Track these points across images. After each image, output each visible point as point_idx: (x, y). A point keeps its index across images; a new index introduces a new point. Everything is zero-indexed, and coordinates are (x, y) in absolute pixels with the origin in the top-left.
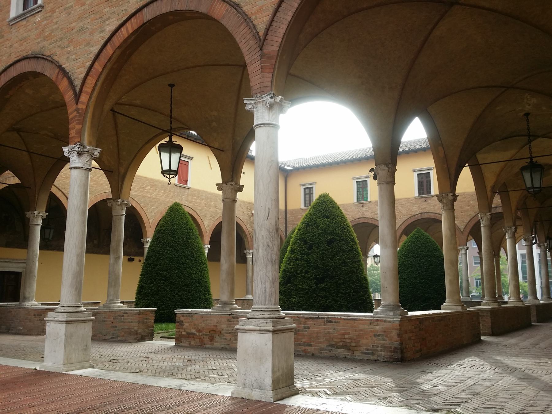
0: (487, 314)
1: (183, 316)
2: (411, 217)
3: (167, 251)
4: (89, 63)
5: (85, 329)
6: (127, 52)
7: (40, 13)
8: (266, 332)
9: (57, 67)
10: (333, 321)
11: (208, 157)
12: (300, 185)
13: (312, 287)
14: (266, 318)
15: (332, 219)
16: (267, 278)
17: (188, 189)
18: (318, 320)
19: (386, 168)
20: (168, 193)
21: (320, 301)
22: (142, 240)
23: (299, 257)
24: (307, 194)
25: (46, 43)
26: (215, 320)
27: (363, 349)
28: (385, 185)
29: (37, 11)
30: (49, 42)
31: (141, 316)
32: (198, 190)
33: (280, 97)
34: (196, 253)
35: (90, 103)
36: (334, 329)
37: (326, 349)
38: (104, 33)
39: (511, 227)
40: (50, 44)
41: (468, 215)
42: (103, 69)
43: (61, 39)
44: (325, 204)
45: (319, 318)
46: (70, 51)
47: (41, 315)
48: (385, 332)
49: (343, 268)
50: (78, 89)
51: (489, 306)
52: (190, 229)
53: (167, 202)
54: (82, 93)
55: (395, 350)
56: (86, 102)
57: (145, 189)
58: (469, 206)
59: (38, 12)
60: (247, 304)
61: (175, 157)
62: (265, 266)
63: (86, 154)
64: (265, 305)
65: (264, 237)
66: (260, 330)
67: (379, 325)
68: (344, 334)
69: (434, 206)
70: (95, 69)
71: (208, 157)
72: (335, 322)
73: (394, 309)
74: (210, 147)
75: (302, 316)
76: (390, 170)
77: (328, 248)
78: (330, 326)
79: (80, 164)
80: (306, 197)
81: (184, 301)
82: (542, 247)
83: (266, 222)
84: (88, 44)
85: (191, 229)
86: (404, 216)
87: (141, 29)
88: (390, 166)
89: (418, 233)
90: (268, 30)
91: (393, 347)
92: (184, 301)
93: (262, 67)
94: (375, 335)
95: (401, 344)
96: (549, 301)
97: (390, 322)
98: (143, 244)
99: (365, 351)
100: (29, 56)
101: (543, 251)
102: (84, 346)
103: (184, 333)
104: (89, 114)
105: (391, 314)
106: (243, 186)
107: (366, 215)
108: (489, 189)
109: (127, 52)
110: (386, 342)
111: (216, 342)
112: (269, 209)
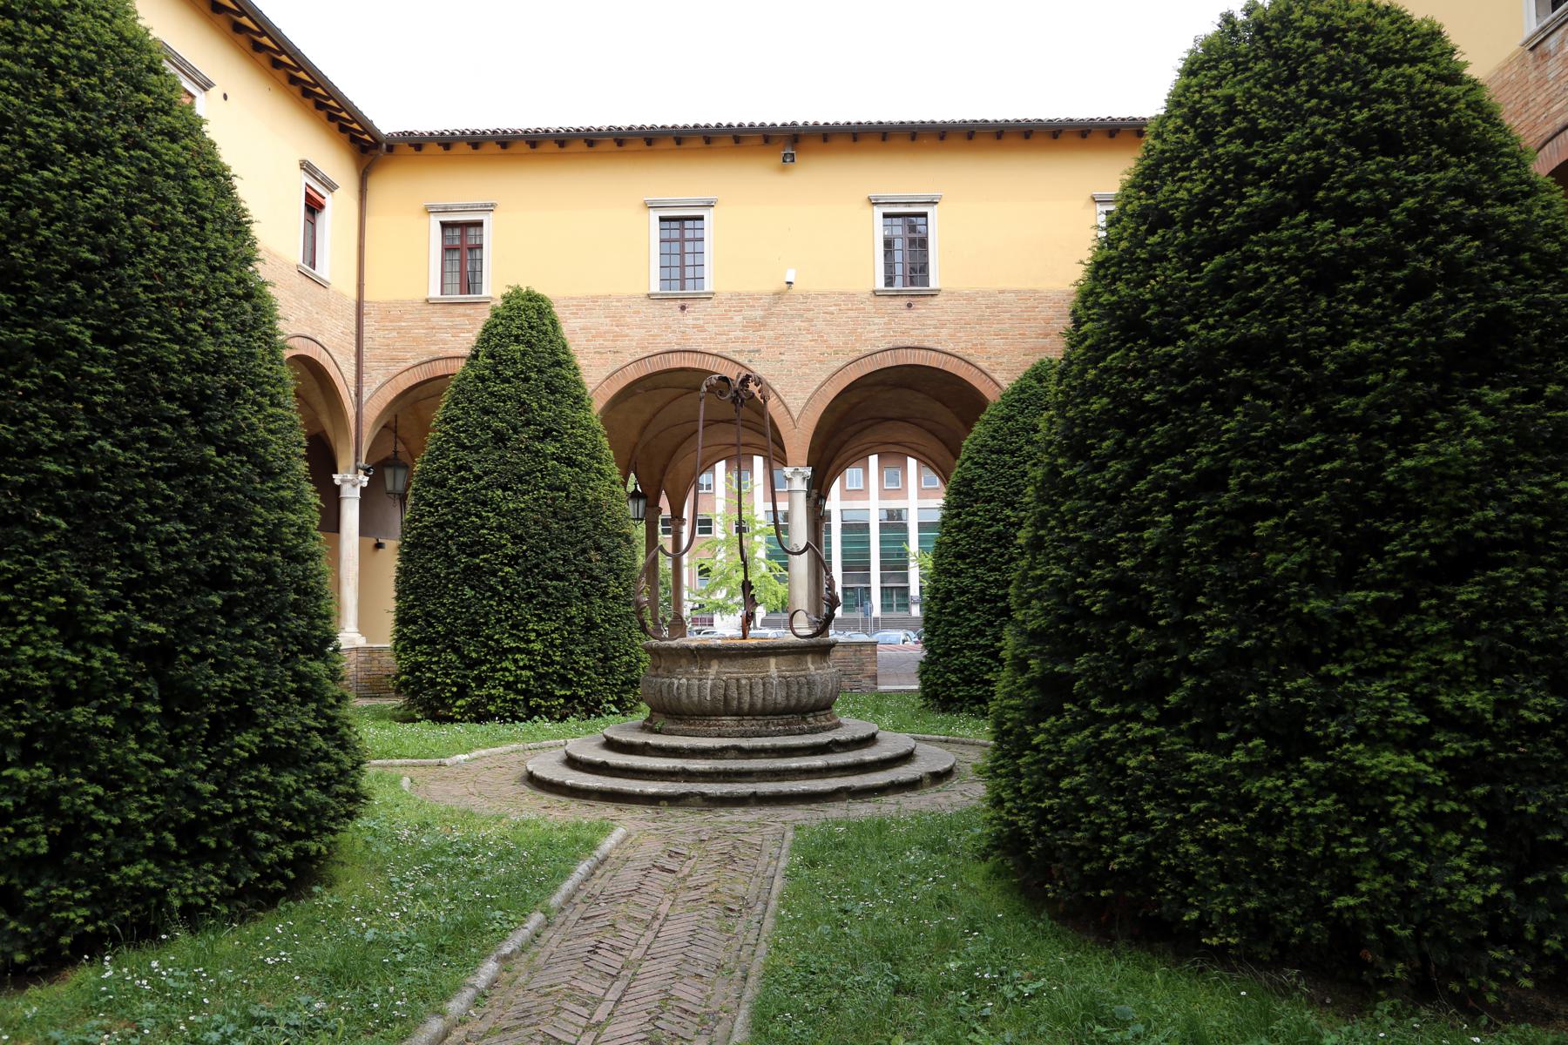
58: (1047, 335)
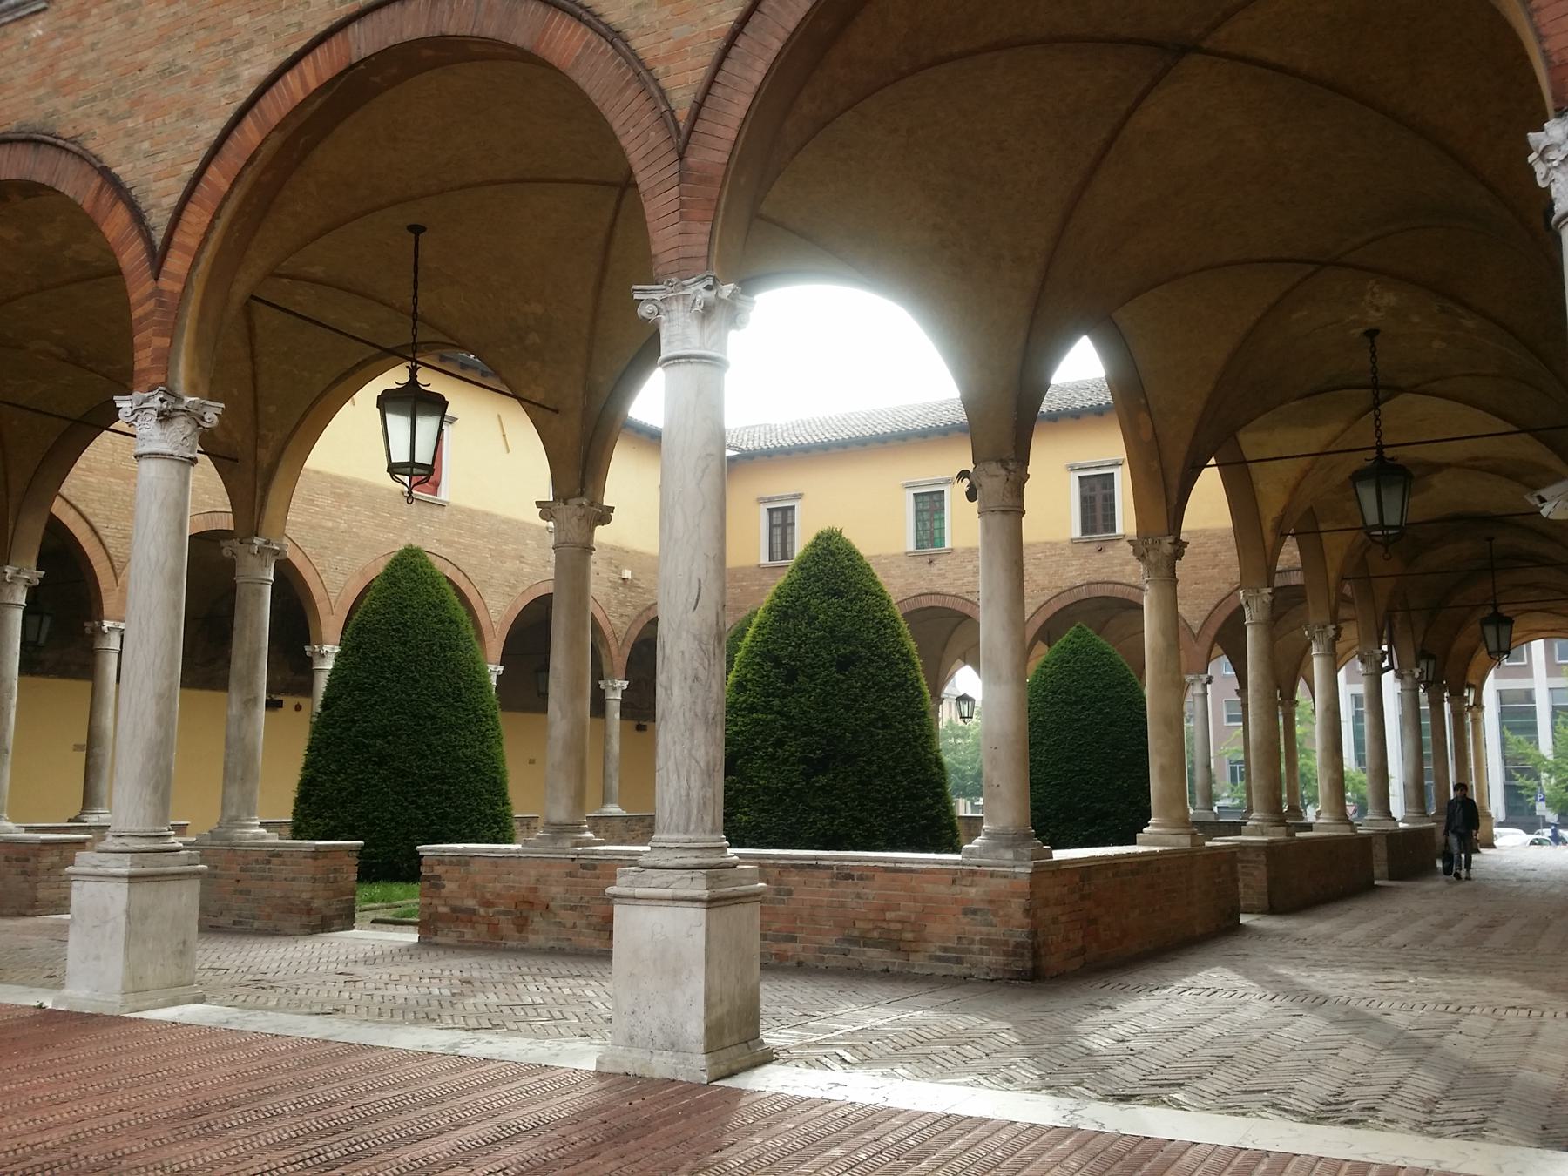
0: (1258, 856)
1: (441, 863)
2: (1060, 594)
3: (383, 682)
4: (194, 166)
5: (180, 896)
6: (302, 141)
7: (42, 15)
8: (689, 904)
9: (97, 172)
10: (856, 874)
11: (499, 416)
12: (758, 499)
13: (795, 783)
14: (689, 866)
15: (851, 601)
16: (693, 762)
17: (440, 508)
18: (816, 873)
19: (1003, 472)
20: (382, 517)
21: (814, 822)
22: (307, 648)
23: (760, 701)
24: (777, 526)
25: (62, 103)
26: (533, 873)
27: (934, 948)
28: (998, 517)
29: (33, 9)
30: (70, 99)
31: (320, 863)
32: (470, 510)
33: (731, 285)
34: (467, 689)
35: (194, 278)
36: (858, 896)
37: (836, 949)
38: (234, 84)
39: (1324, 627)
40: (75, 107)
41: (1212, 592)
42: (233, 185)
43: (107, 94)
44: (832, 559)
45: (817, 867)
46: (136, 130)
47: (27, 860)
48: (991, 902)
49: (878, 734)
50: (158, 237)
51: (1263, 834)
52: (451, 622)
53: (381, 543)
54: (171, 250)
55: (1016, 951)
56: (184, 273)
57: (317, 506)
58: (1214, 567)
59: (37, 12)
60: (642, 827)
61: (427, 426)
62: (688, 733)
63: (183, 419)
64: (686, 831)
65: (687, 655)
66: (674, 899)
67: (976, 885)
68: (883, 910)
69: (1121, 565)
70: (208, 183)
71: (499, 416)
72: (861, 878)
73: (1017, 843)
74: (521, 400)
75: (771, 861)
76: (1012, 477)
77: (838, 680)
78: (846, 888)
79: (165, 445)
80: (774, 533)
81: (432, 823)
82: (1408, 679)
83: (692, 616)
84: (189, 113)
85: (456, 622)
86: (1043, 590)
87: (344, 79)
88: (1011, 466)
89: (1079, 638)
90: (699, 106)
91: (1012, 941)
92: (432, 823)
93: (682, 204)
94: (966, 912)
95: (1034, 933)
96: (1420, 823)
97: (1006, 877)
98: (310, 661)
99: (938, 953)
100: (10, 136)
101: (1410, 690)
102: (178, 944)
103: (442, 909)
104: (190, 309)
105: (1009, 855)
106: (611, 509)
107: (941, 586)
108: (1268, 525)
109: (302, 141)
110: (993, 930)
111: (536, 932)
112: (700, 581)
